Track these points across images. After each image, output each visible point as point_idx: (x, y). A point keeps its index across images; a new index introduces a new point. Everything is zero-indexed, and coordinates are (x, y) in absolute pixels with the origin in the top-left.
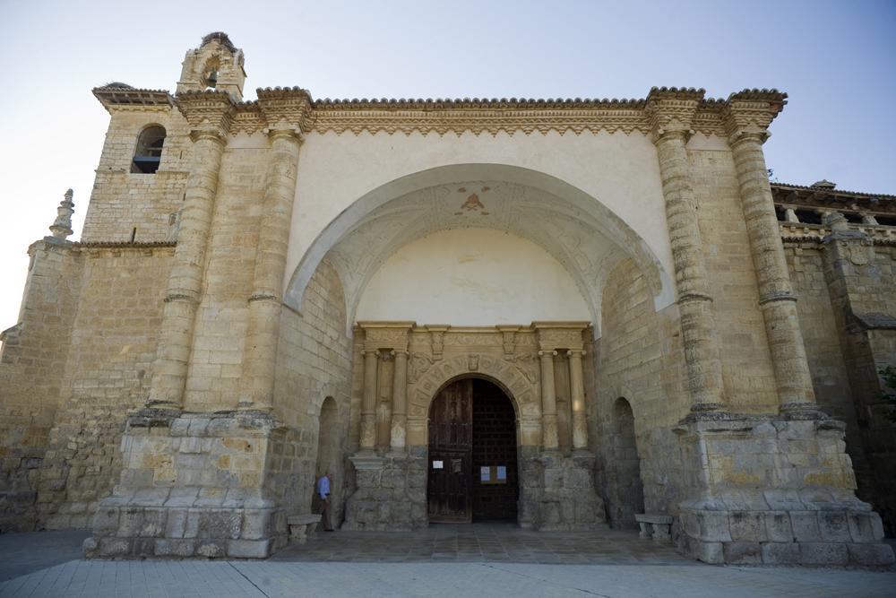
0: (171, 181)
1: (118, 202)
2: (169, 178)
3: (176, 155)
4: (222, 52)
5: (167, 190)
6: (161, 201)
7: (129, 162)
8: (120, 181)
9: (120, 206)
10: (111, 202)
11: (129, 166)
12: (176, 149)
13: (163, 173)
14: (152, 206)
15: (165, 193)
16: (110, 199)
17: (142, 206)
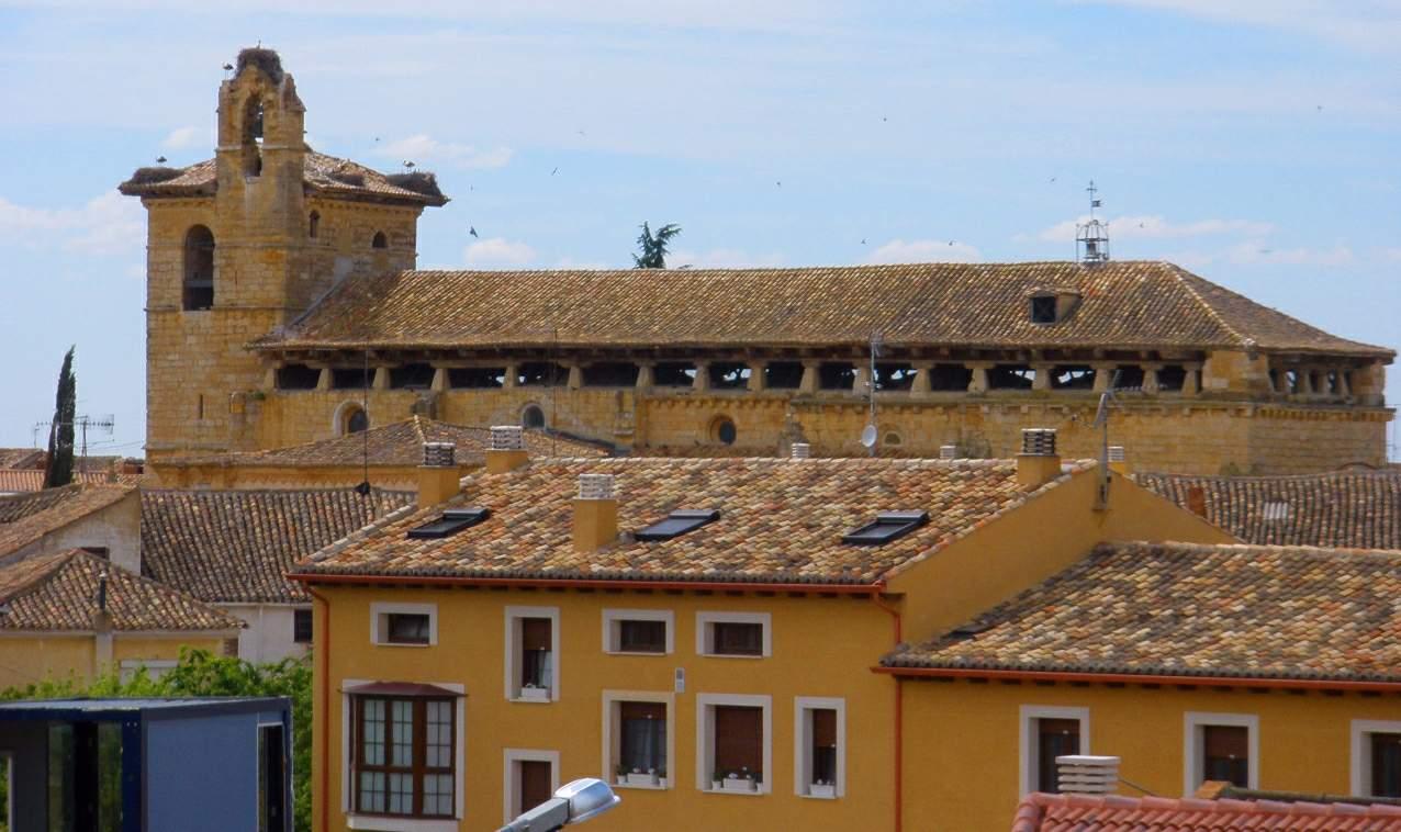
0: (230, 322)
1: (177, 357)
2: (227, 318)
3: (231, 279)
4: (263, 85)
5: (228, 337)
6: (224, 354)
7: (179, 293)
8: (174, 324)
9: (181, 364)
10: (171, 357)
11: (180, 299)
12: (229, 269)
13: (219, 310)
14: (214, 362)
15: (226, 342)
16: (168, 354)
17: (202, 363)
